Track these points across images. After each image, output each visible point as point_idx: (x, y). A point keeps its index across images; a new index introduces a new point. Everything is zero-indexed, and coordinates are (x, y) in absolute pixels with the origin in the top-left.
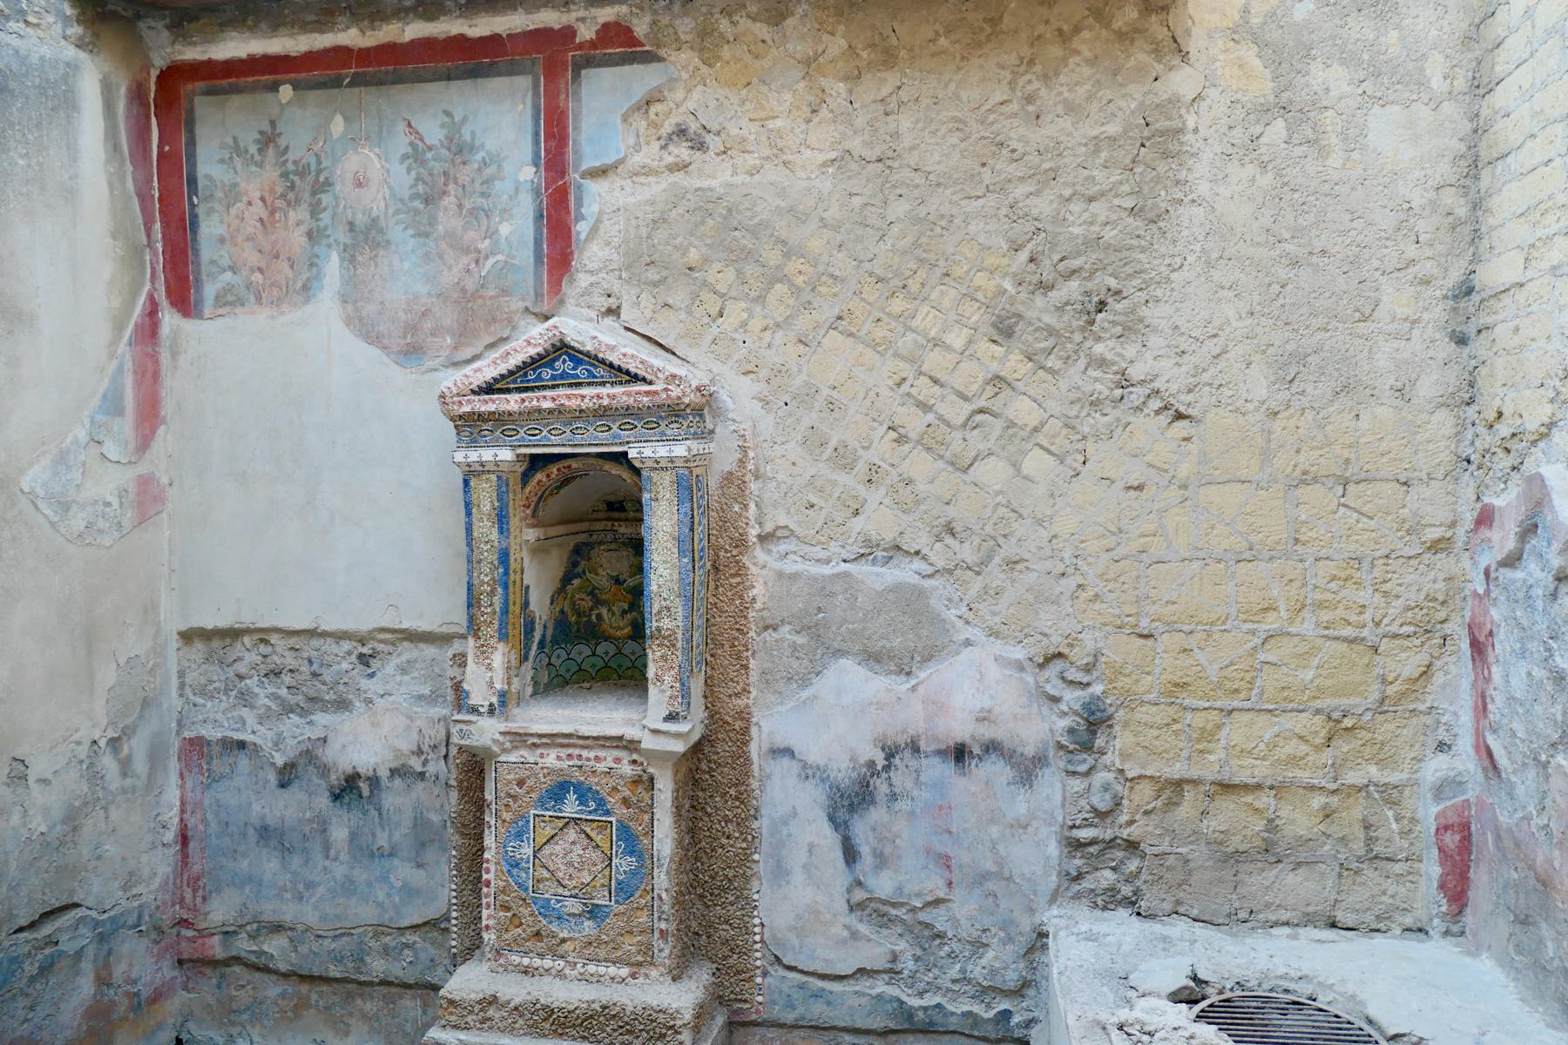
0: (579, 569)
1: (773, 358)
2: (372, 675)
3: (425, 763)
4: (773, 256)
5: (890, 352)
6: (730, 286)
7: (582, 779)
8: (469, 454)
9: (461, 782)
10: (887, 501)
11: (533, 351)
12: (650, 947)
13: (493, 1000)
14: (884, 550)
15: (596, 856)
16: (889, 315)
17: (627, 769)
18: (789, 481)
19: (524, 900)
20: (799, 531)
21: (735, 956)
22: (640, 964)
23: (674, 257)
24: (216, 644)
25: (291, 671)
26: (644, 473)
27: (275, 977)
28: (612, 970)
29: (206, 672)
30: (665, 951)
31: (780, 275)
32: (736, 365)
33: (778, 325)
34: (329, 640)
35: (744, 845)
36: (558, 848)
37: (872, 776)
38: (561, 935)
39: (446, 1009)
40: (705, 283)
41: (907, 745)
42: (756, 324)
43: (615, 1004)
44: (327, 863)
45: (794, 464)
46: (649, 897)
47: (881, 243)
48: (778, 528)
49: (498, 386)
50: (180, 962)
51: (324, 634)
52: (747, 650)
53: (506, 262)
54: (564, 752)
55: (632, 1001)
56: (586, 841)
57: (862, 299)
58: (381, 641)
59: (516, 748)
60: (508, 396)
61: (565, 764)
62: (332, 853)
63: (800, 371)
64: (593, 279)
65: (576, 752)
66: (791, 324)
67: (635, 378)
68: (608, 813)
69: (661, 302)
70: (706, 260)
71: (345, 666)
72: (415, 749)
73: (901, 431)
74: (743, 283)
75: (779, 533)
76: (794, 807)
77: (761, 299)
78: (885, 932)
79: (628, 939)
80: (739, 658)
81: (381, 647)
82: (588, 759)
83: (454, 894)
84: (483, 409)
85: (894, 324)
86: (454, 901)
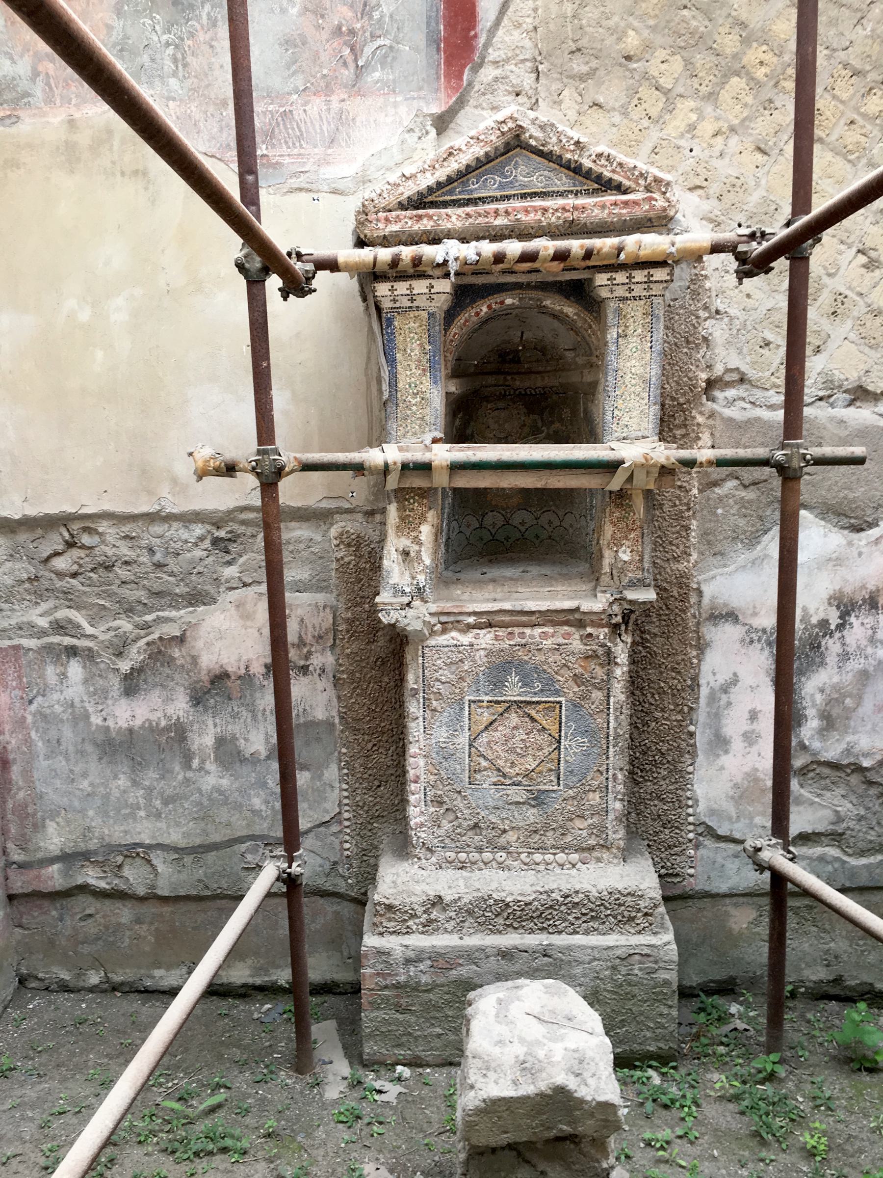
0: (469, 431)
1: (725, 169)
2: (229, 563)
3: (307, 657)
4: (729, 43)
5: (864, 161)
6: (677, 80)
7: (526, 658)
8: (397, 285)
9: (353, 673)
10: (852, 336)
11: (479, 151)
12: (602, 829)
13: (438, 902)
14: (845, 392)
15: (542, 739)
16: (864, 116)
17: (576, 644)
18: (742, 316)
19: (459, 792)
20: (751, 373)
21: (667, 831)
22: (591, 849)
23: (608, 42)
24: (23, 537)
25: (126, 563)
26: (613, 305)
27: (129, 904)
28: (561, 857)
29: (11, 572)
30: (617, 835)
31: (737, 66)
32: (681, 179)
33: (733, 129)
34: (175, 525)
35: (679, 717)
36: (497, 734)
37: (824, 636)
38: (502, 827)
39: (381, 915)
40: (645, 76)
41: (864, 600)
42: (707, 128)
43: (577, 892)
44: (190, 774)
45: (748, 296)
46: (603, 778)
47: (859, 27)
48: (728, 371)
49: (430, 199)
50: (11, 898)
51: (170, 518)
52: (689, 509)
53: (391, 47)
54: (501, 633)
55: (594, 886)
56: (530, 725)
57: (834, 97)
58: (243, 523)
59: (444, 631)
60: (449, 211)
61: (506, 644)
62: (195, 763)
63: (757, 185)
64: (498, 72)
65: (517, 630)
66: (748, 127)
67: (606, 185)
68: (557, 693)
69: (589, 101)
70: (648, 47)
71: (198, 553)
72: (296, 641)
73: (873, 254)
74: (692, 76)
75: (727, 378)
76: (735, 674)
77: (712, 97)
78: (828, 794)
79: (578, 823)
80: (680, 516)
81: (241, 529)
82: (532, 637)
83: (346, 794)
84: (416, 228)
85: (869, 127)
86: (346, 801)
